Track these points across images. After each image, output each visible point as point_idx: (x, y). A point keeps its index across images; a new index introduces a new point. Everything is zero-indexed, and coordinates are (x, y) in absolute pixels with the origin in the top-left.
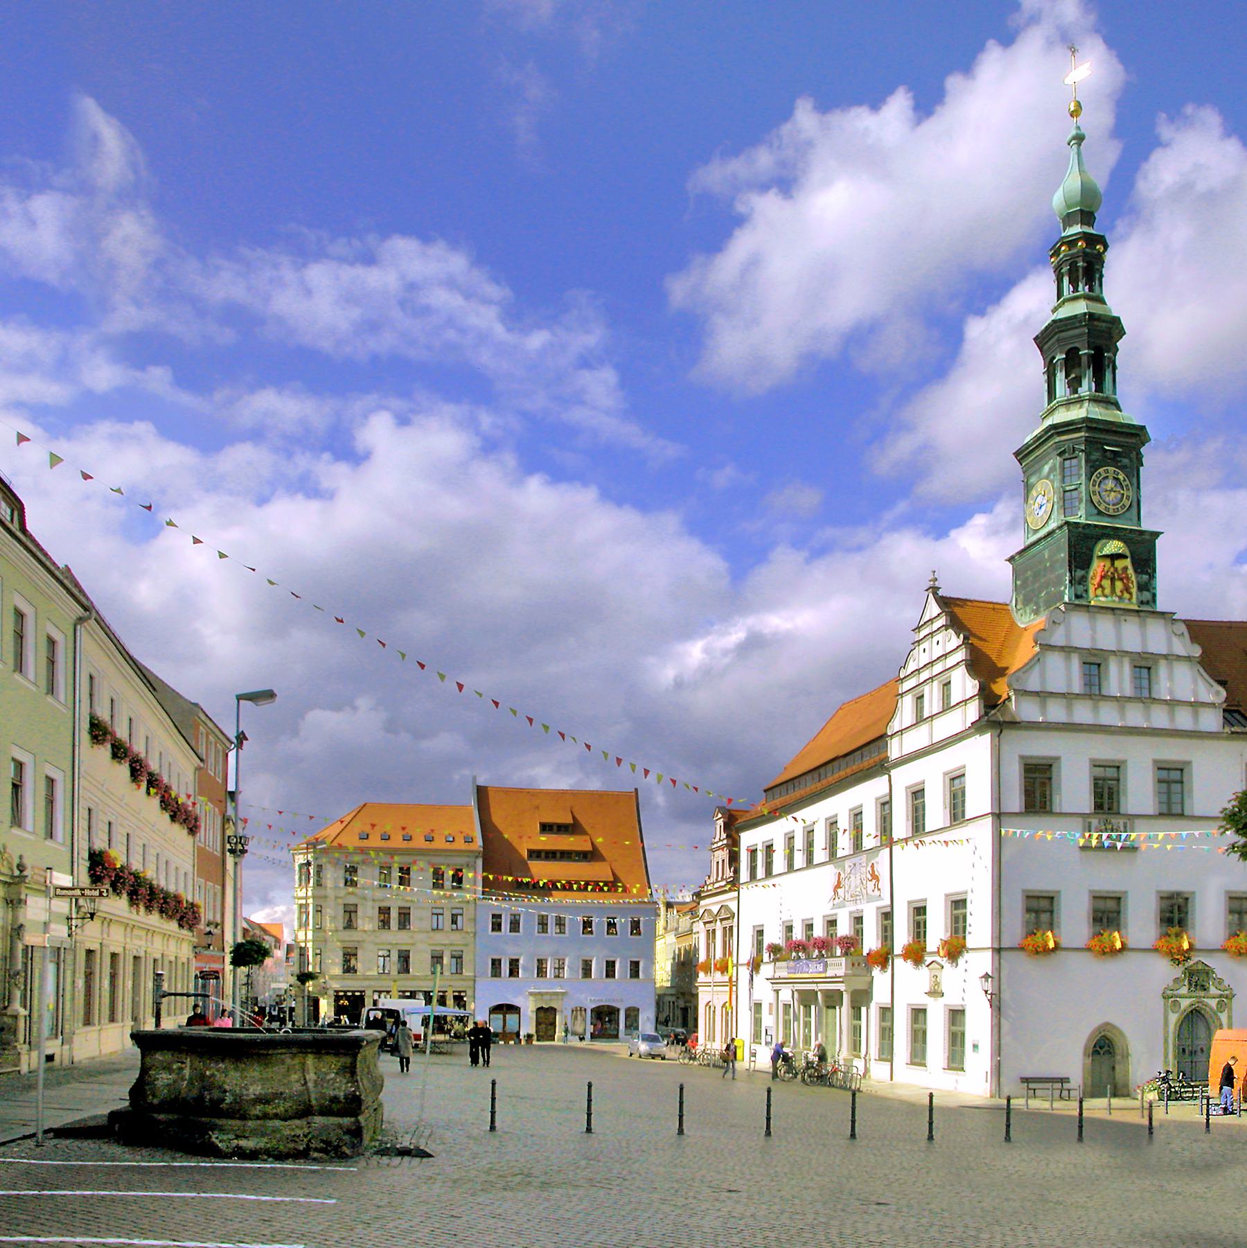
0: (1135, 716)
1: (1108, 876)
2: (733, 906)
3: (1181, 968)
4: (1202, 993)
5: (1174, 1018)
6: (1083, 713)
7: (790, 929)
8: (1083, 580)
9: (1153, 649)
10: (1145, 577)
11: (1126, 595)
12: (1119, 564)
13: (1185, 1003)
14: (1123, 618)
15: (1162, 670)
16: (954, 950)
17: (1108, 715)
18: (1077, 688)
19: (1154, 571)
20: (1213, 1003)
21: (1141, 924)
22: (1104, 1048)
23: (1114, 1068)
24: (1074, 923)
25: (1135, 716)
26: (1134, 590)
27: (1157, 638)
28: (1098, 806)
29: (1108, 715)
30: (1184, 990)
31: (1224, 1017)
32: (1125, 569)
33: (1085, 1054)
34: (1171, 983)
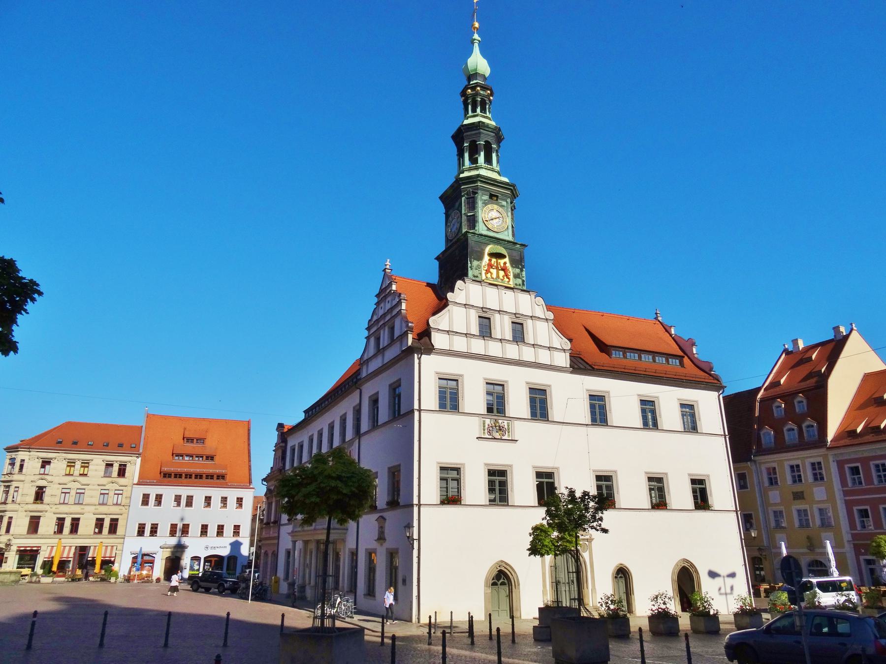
0: (512, 351)
1: (498, 454)
8: (479, 267)
10: (518, 271)
12: (502, 261)
17: (494, 349)
18: (475, 330)
21: (523, 489)
24: (475, 487)
25: (512, 351)
26: (511, 277)
27: (527, 304)
28: (490, 410)
29: (494, 349)
32: (505, 263)
33: (486, 585)
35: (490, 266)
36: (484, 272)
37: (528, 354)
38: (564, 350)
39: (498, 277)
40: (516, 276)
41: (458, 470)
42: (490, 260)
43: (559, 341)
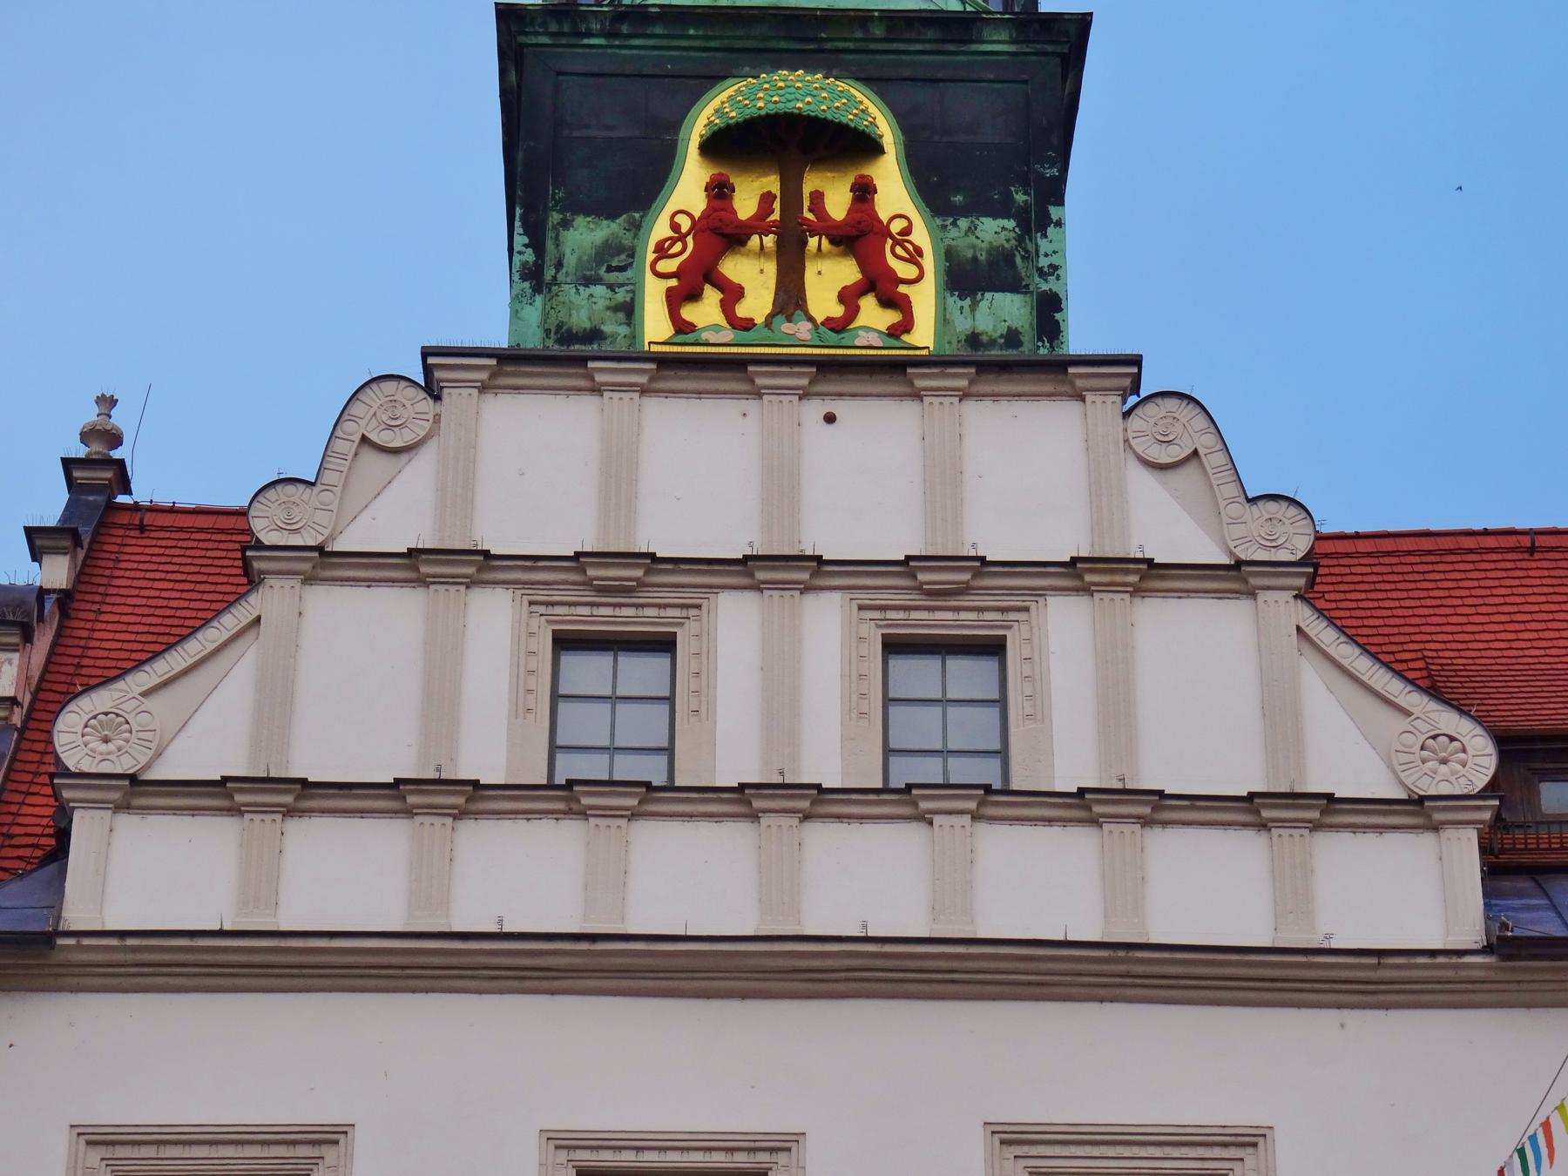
0: (868, 883)
6: (523, 879)
9: (996, 536)
11: (874, 316)
14: (815, 409)
15: (1062, 631)
17: (689, 881)
19: (1055, 192)
32: (864, 192)
35: (720, 232)
36: (654, 295)
37: (1036, 886)
38: (1417, 811)
39: (790, 297)
40: (964, 279)
42: (719, 191)
43: (1358, 731)
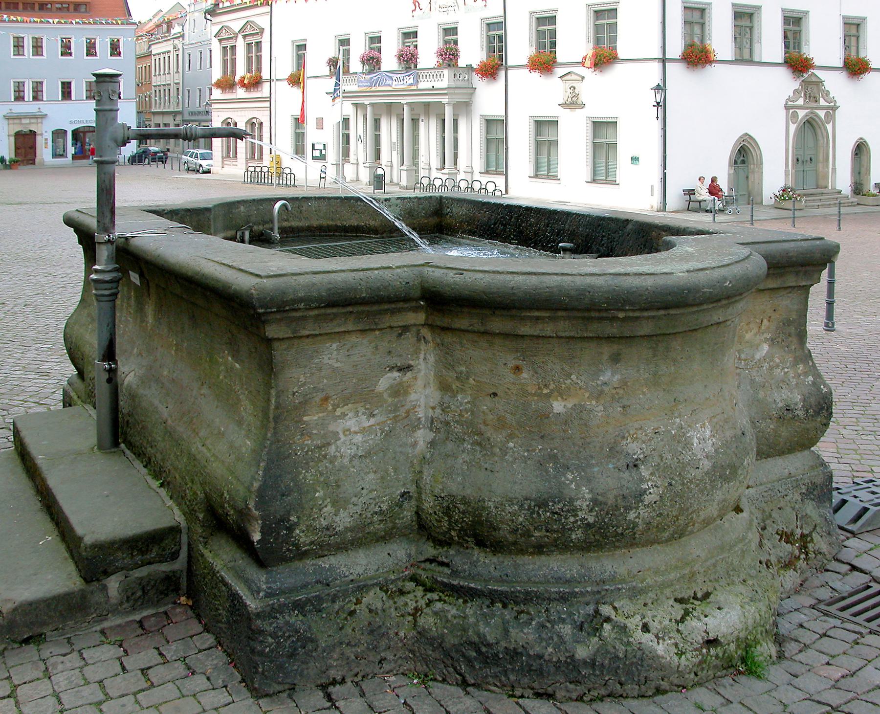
2: (263, 22)
3: (798, 82)
4: (814, 105)
5: (793, 128)
7: (344, 42)
13: (801, 113)
16: (604, 58)
20: (822, 114)
22: (744, 155)
23: (747, 177)
30: (801, 102)
31: (829, 127)
34: (792, 95)
41: (702, 11)
